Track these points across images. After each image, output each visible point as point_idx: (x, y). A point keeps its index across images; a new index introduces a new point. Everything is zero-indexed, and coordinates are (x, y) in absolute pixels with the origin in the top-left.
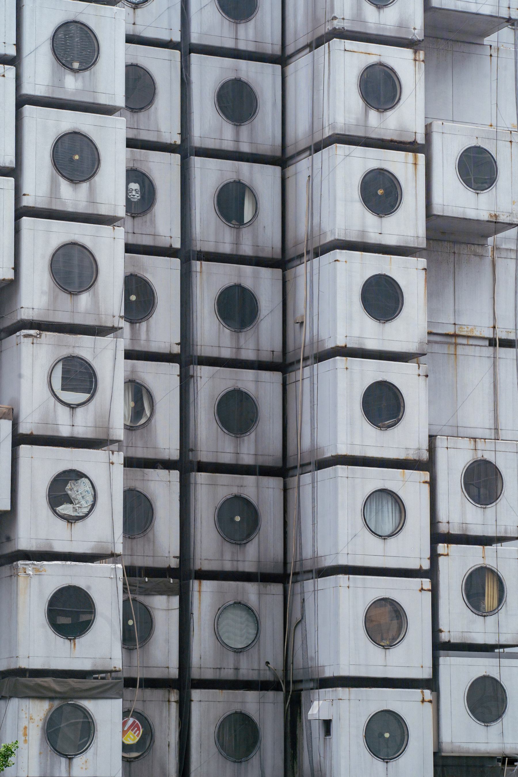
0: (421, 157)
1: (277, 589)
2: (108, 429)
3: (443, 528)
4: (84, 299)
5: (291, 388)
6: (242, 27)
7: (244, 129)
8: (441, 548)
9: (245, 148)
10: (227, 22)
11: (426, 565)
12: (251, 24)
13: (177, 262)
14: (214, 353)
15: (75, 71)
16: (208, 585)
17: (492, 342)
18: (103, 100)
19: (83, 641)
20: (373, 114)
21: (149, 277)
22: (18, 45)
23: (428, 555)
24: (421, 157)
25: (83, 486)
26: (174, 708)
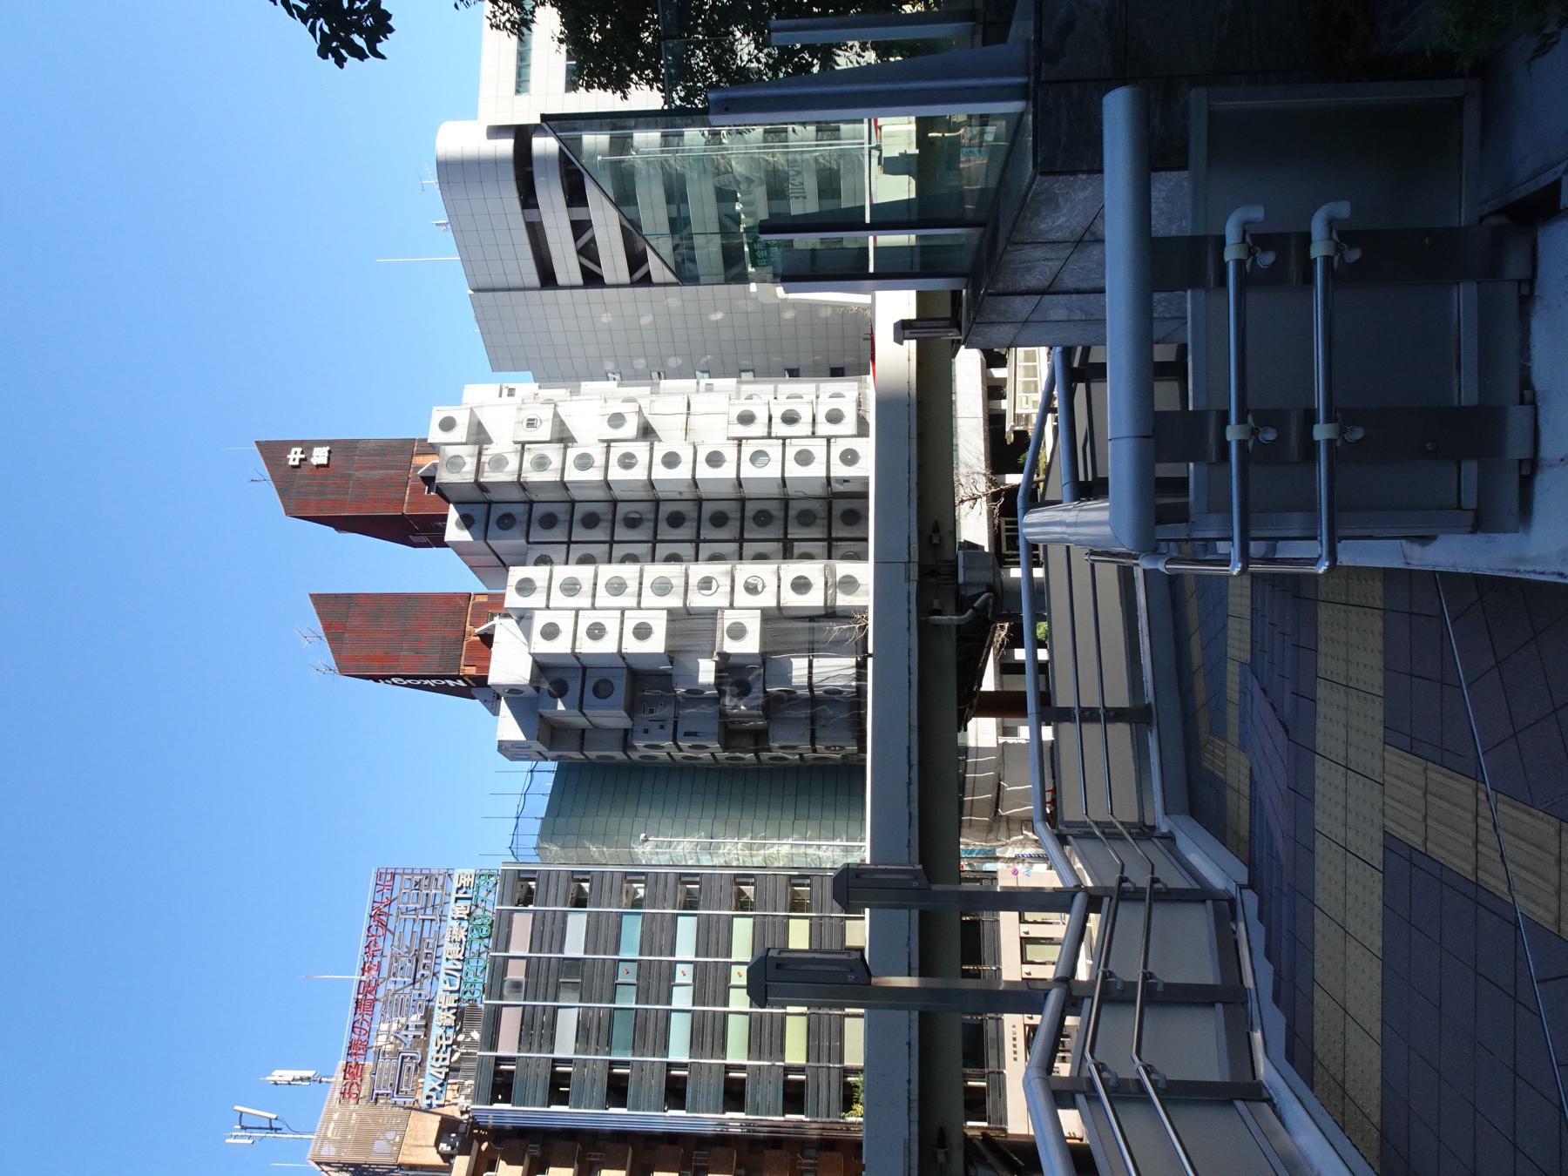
0: (612, 444)
1: (792, 503)
2: (727, 573)
3: (765, 434)
4: (674, 582)
5: (711, 496)
7: (602, 517)
8: (773, 435)
11: (781, 441)
13: (658, 545)
14: (695, 530)
15: (580, 588)
16: (789, 531)
17: (688, 414)
18: (592, 575)
19: (812, 580)
20: (594, 465)
21: (664, 556)
22: (571, 609)
23: (776, 440)
25: (750, 581)
26: (839, 543)
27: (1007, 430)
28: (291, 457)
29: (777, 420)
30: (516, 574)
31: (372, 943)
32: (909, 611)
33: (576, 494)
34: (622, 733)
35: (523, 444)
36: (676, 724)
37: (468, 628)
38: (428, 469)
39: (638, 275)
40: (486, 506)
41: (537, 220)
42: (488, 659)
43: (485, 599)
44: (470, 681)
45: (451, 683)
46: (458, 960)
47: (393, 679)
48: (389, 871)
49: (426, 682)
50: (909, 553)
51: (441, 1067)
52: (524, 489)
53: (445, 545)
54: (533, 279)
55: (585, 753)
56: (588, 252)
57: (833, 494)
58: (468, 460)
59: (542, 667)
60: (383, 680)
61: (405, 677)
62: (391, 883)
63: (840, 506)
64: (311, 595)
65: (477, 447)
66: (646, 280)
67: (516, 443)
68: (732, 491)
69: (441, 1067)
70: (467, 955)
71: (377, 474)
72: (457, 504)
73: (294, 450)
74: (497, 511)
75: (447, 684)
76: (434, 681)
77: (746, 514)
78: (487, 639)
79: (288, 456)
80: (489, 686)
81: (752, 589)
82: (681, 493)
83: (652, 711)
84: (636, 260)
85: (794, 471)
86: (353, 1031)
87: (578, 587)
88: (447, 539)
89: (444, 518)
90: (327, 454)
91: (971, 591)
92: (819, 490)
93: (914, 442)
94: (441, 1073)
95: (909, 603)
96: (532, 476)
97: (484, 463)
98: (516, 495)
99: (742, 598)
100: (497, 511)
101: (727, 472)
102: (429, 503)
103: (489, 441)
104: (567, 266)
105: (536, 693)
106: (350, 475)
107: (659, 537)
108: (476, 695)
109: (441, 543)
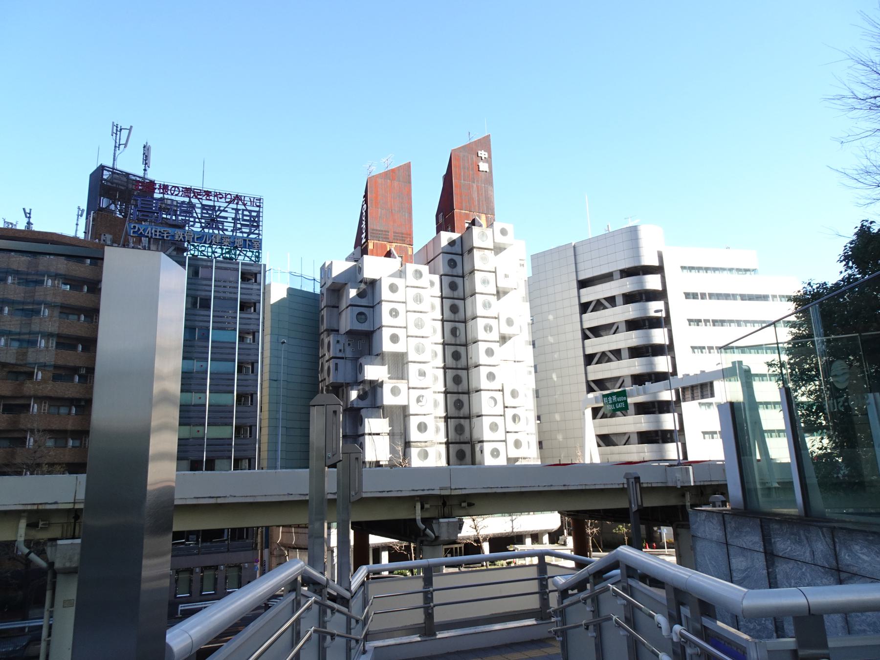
1: (468, 420)
6: (455, 292)
7: (456, 315)
9: (457, 320)
10: (451, 291)
11: (502, 414)
12: (457, 291)
16: (452, 420)
24: (497, 320)
27: (515, 546)
28: (483, 152)
29: (513, 411)
30: (425, 269)
31: (221, 196)
32: (423, 490)
33: (469, 301)
34: (336, 328)
35: (495, 272)
36: (342, 358)
37: (394, 244)
38: (479, 222)
39: (588, 333)
41: (614, 278)
42: (377, 255)
43: (410, 253)
44: (364, 246)
45: (364, 236)
46: (212, 242)
48: (261, 204)
49: (364, 223)
50: (456, 489)
51: (152, 233)
52: (470, 273)
53: (438, 231)
54: (582, 277)
55: (325, 309)
56: (599, 305)
57: (474, 444)
59: (373, 284)
60: (365, 200)
61: (366, 212)
62: (255, 205)
63: (467, 448)
64: (410, 163)
66: (585, 337)
67: (496, 268)
68: (473, 387)
69: (152, 233)
70: (214, 246)
71: (475, 196)
72: (461, 237)
73: (486, 153)
74: (458, 259)
76: (364, 227)
77: (461, 395)
78: (389, 254)
80: (362, 256)
81: (418, 400)
82: (471, 358)
83: (349, 344)
84: (597, 331)
85: (486, 422)
86: (173, 187)
87: (418, 303)
88: (443, 233)
89: (453, 231)
91: (435, 526)
92: (476, 436)
93: (518, 490)
94: (148, 233)
95: (428, 490)
96: (478, 276)
98: (467, 269)
99: (414, 394)
100: (458, 259)
101: (484, 383)
102: (461, 223)
103: (496, 253)
104: (591, 294)
105: (359, 281)
106: (474, 182)
107: (446, 346)
109: (438, 230)
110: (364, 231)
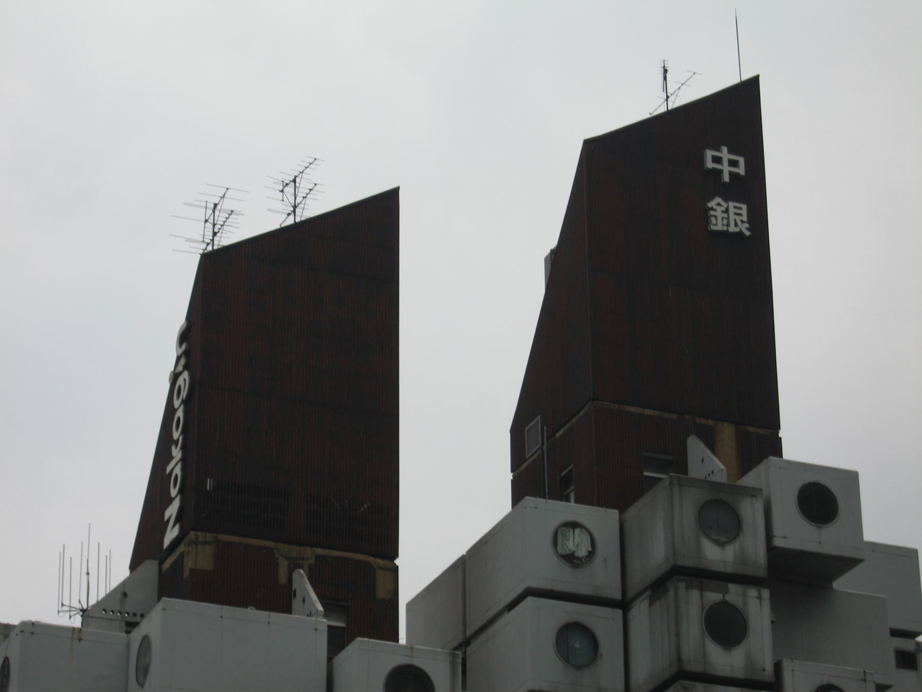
28: (725, 154)
37: (311, 553)
40: (618, 596)
47: (186, 375)
49: (177, 453)
53: (517, 497)
58: (730, 552)
60: (186, 353)
65: (762, 573)
67: (778, 667)
73: (741, 160)
75: (170, 500)
76: (178, 471)
79: (725, 149)
90: (732, 229)
97: (726, 591)
108: (141, 569)
110: (174, 492)
